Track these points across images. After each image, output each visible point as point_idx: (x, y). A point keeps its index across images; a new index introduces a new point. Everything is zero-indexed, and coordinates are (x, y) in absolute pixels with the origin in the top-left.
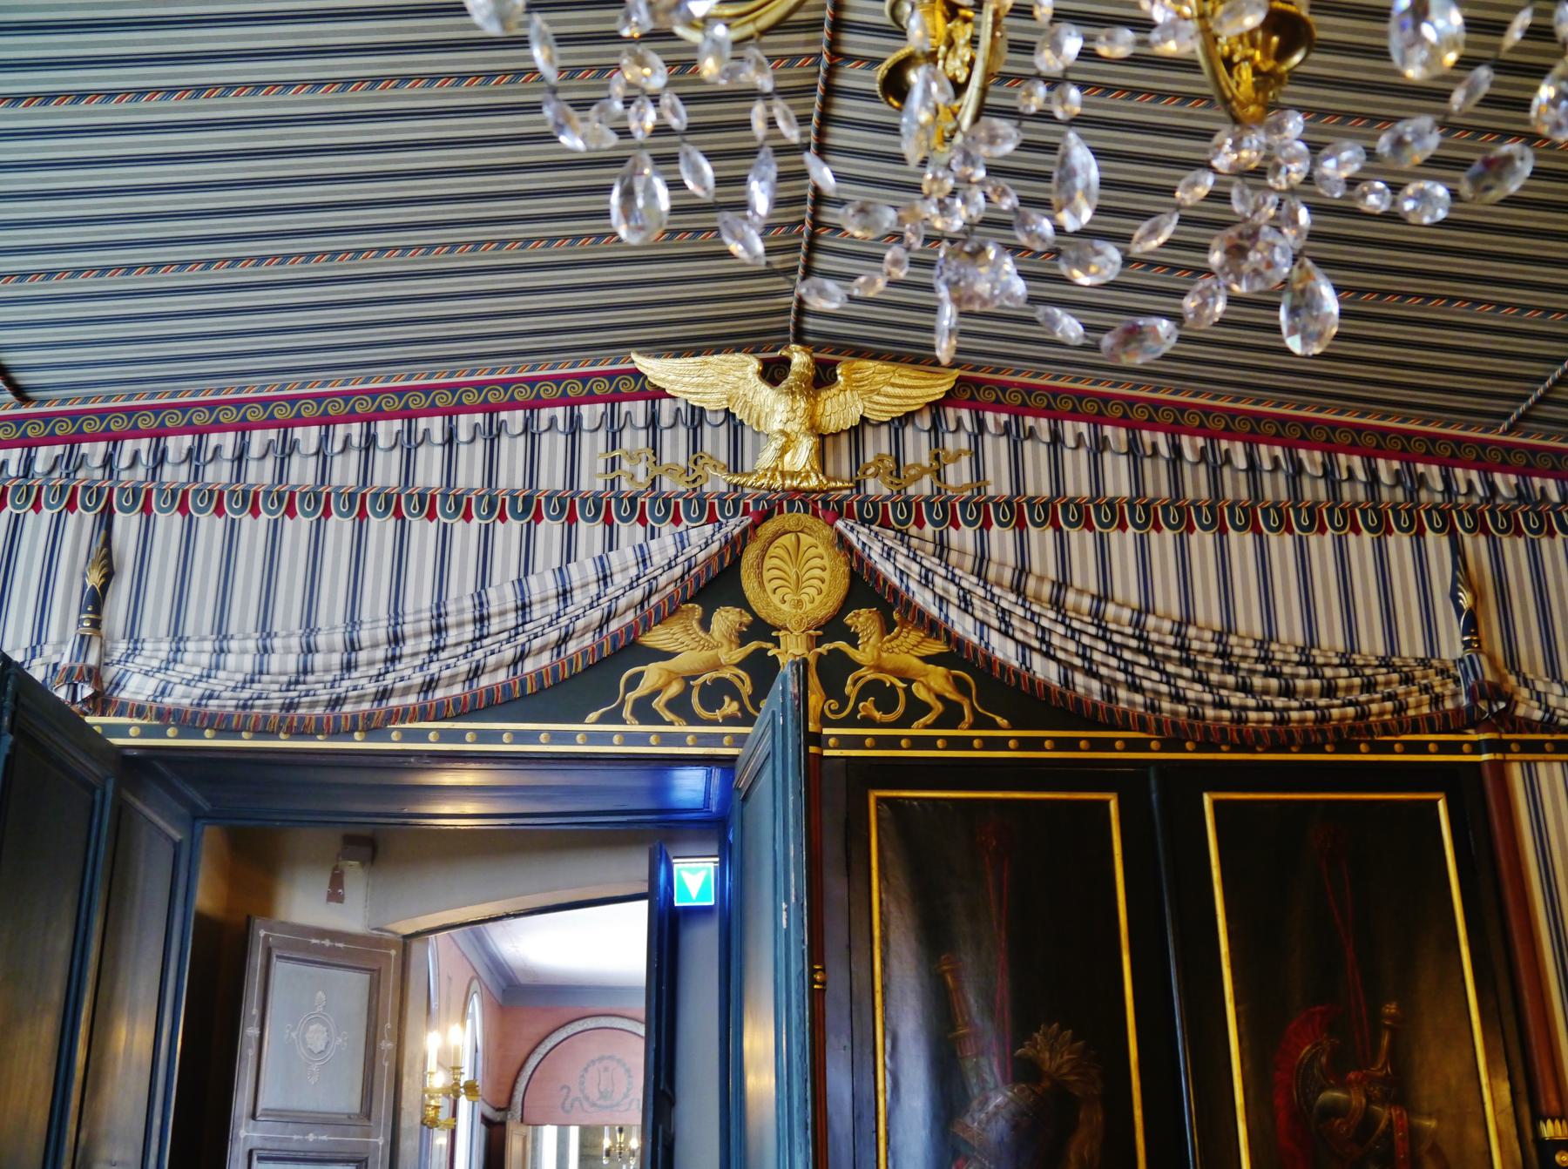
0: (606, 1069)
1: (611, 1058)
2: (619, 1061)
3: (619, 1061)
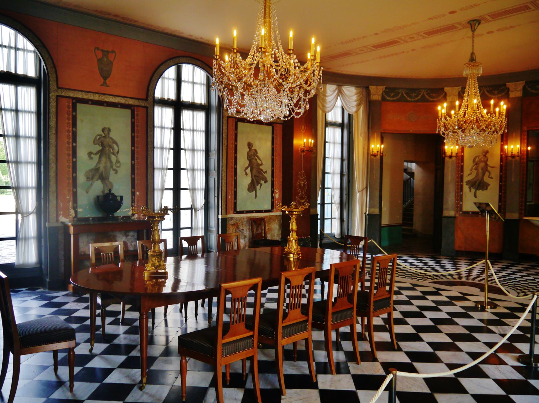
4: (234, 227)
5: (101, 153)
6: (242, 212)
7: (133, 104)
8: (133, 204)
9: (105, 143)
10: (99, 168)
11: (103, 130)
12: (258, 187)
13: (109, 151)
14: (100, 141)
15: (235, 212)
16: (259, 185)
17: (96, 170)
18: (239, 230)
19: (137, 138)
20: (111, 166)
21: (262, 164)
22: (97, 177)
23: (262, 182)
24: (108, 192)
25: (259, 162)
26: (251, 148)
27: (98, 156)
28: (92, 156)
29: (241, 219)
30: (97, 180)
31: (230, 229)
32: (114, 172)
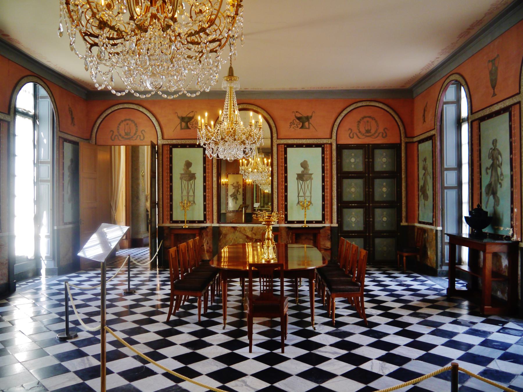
0: (127, 124)
1: (129, 120)
2: (132, 121)
3: (132, 121)
7: (509, 104)
8: (512, 222)
9: (494, 156)
11: (493, 144)
13: (496, 163)
19: (514, 143)
20: (498, 180)
30: (491, 195)
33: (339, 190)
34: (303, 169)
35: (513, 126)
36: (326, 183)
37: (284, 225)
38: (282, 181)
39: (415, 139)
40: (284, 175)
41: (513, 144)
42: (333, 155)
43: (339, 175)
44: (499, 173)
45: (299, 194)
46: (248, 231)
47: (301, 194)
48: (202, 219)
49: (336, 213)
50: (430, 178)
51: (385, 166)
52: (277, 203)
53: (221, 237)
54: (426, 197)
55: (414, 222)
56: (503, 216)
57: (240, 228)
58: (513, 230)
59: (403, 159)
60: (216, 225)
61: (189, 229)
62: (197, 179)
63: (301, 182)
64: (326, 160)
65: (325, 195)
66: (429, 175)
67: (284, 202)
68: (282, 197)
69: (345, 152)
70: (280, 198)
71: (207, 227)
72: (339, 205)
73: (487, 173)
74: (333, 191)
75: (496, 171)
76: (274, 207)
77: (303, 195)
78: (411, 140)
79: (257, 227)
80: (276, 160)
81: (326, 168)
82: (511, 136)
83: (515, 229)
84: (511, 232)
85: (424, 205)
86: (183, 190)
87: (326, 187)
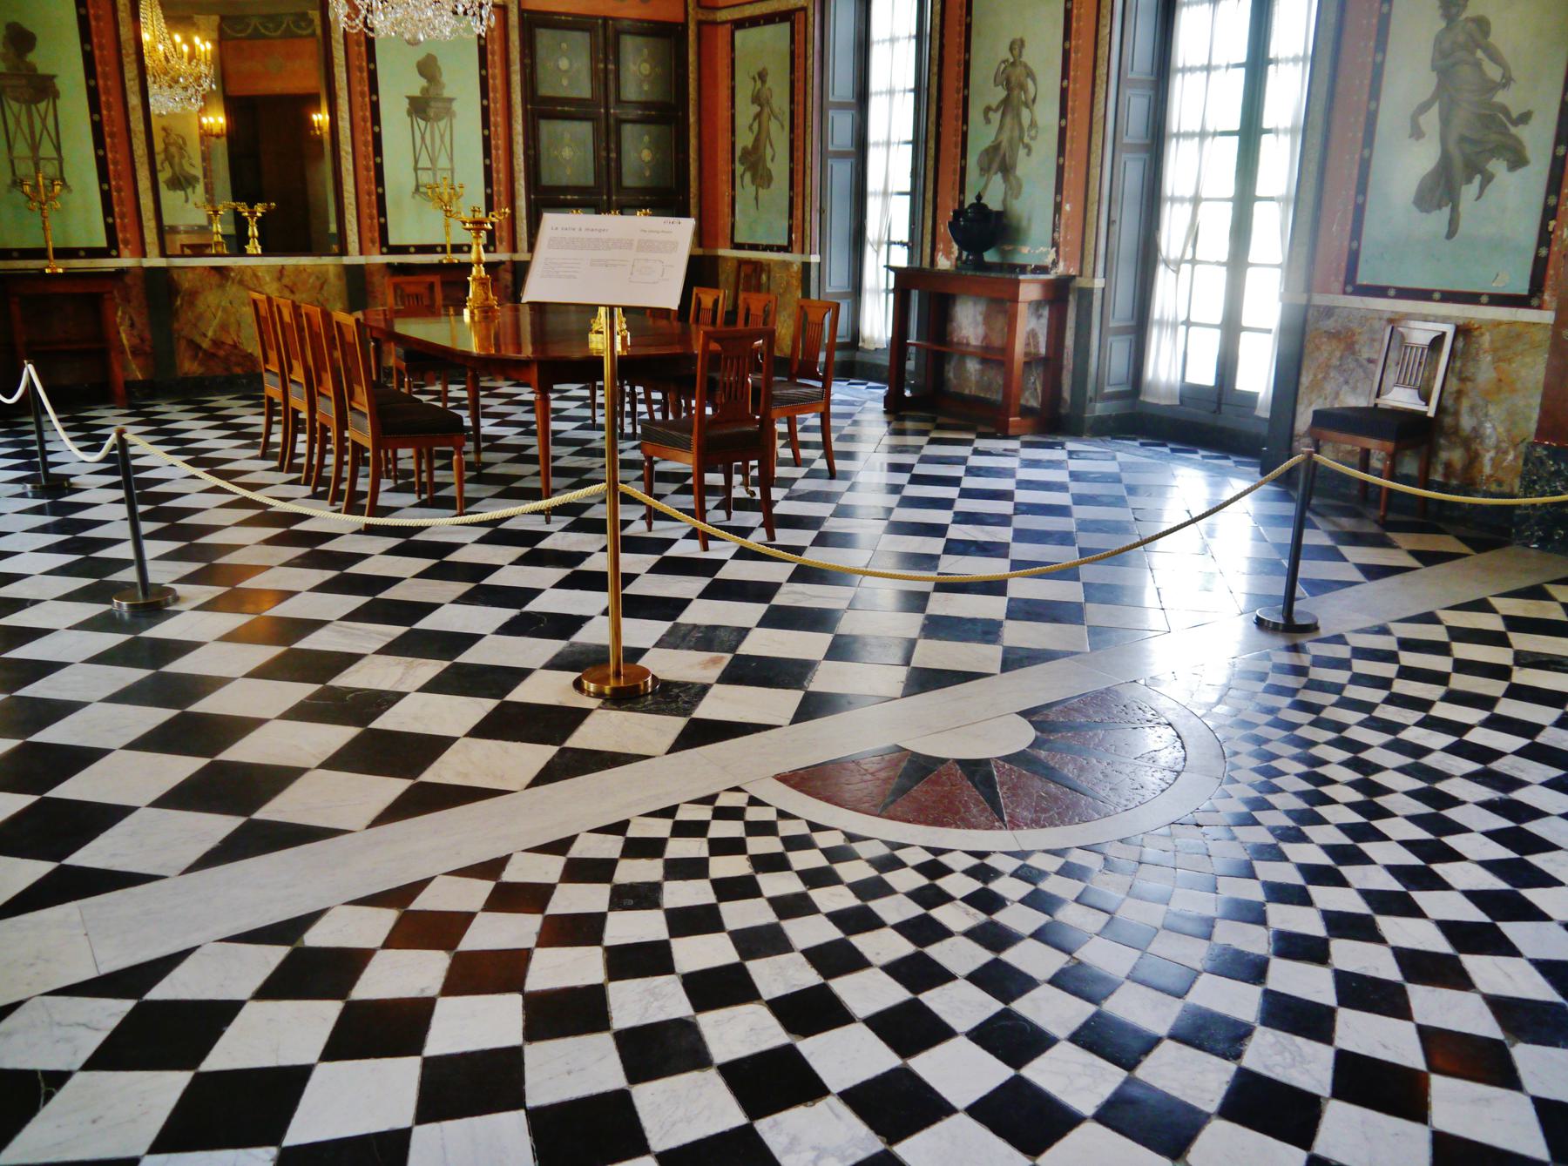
4: (1334, 343)
5: (1006, 102)
6: (1380, 291)
8: (1056, 235)
9: (1013, 79)
10: (1000, 144)
11: (1011, 49)
12: (1469, 192)
13: (1019, 97)
14: (1004, 75)
15: (1349, 289)
16: (1477, 179)
17: (995, 148)
18: (1357, 360)
19: (1076, 53)
20: (1021, 139)
21: (1507, 81)
22: (995, 166)
23: (1498, 166)
24: (975, 201)
25: (1493, 72)
26: (1458, 14)
27: (1000, 112)
28: (991, 115)
29: (1367, 320)
30: (996, 173)
31: (1318, 348)
32: (1026, 151)
33: (531, 152)
34: (423, 82)
35: (1075, 11)
36: (493, 129)
37: (380, 259)
38: (364, 120)
39: (723, 15)
40: (367, 99)
41: (1073, 55)
42: (511, 44)
43: (529, 107)
44: (1026, 121)
45: (416, 162)
46: (268, 279)
47: (424, 162)
48: (101, 242)
49: (525, 221)
50: (782, 126)
51: (646, 87)
52: (353, 190)
53: (179, 302)
54: (762, 178)
55: (716, 247)
56: (1029, 219)
57: (241, 270)
58: (1057, 252)
59: (691, 68)
60: (154, 261)
61: (69, 275)
62: (62, 95)
63: (422, 123)
64: (490, 57)
65: (491, 164)
66: (776, 118)
67: (373, 187)
68: (368, 169)
69: (544, 37)
70: (362, 173)
71: (121, 272)
72: (532, 197)
73: (988, 121)
74: (516, 156)
75: (1018, 116)
76: (346, 201)
77: (429, 166)
78: (711, 17)
79: (296, 267)
80: (343, 47)
81: (491, 81)
82: (1067, 35)
83: (1062, 248)
84: (1052, 256)
85: (756, 199)
86: (11, 136)
87: (493, 142)
